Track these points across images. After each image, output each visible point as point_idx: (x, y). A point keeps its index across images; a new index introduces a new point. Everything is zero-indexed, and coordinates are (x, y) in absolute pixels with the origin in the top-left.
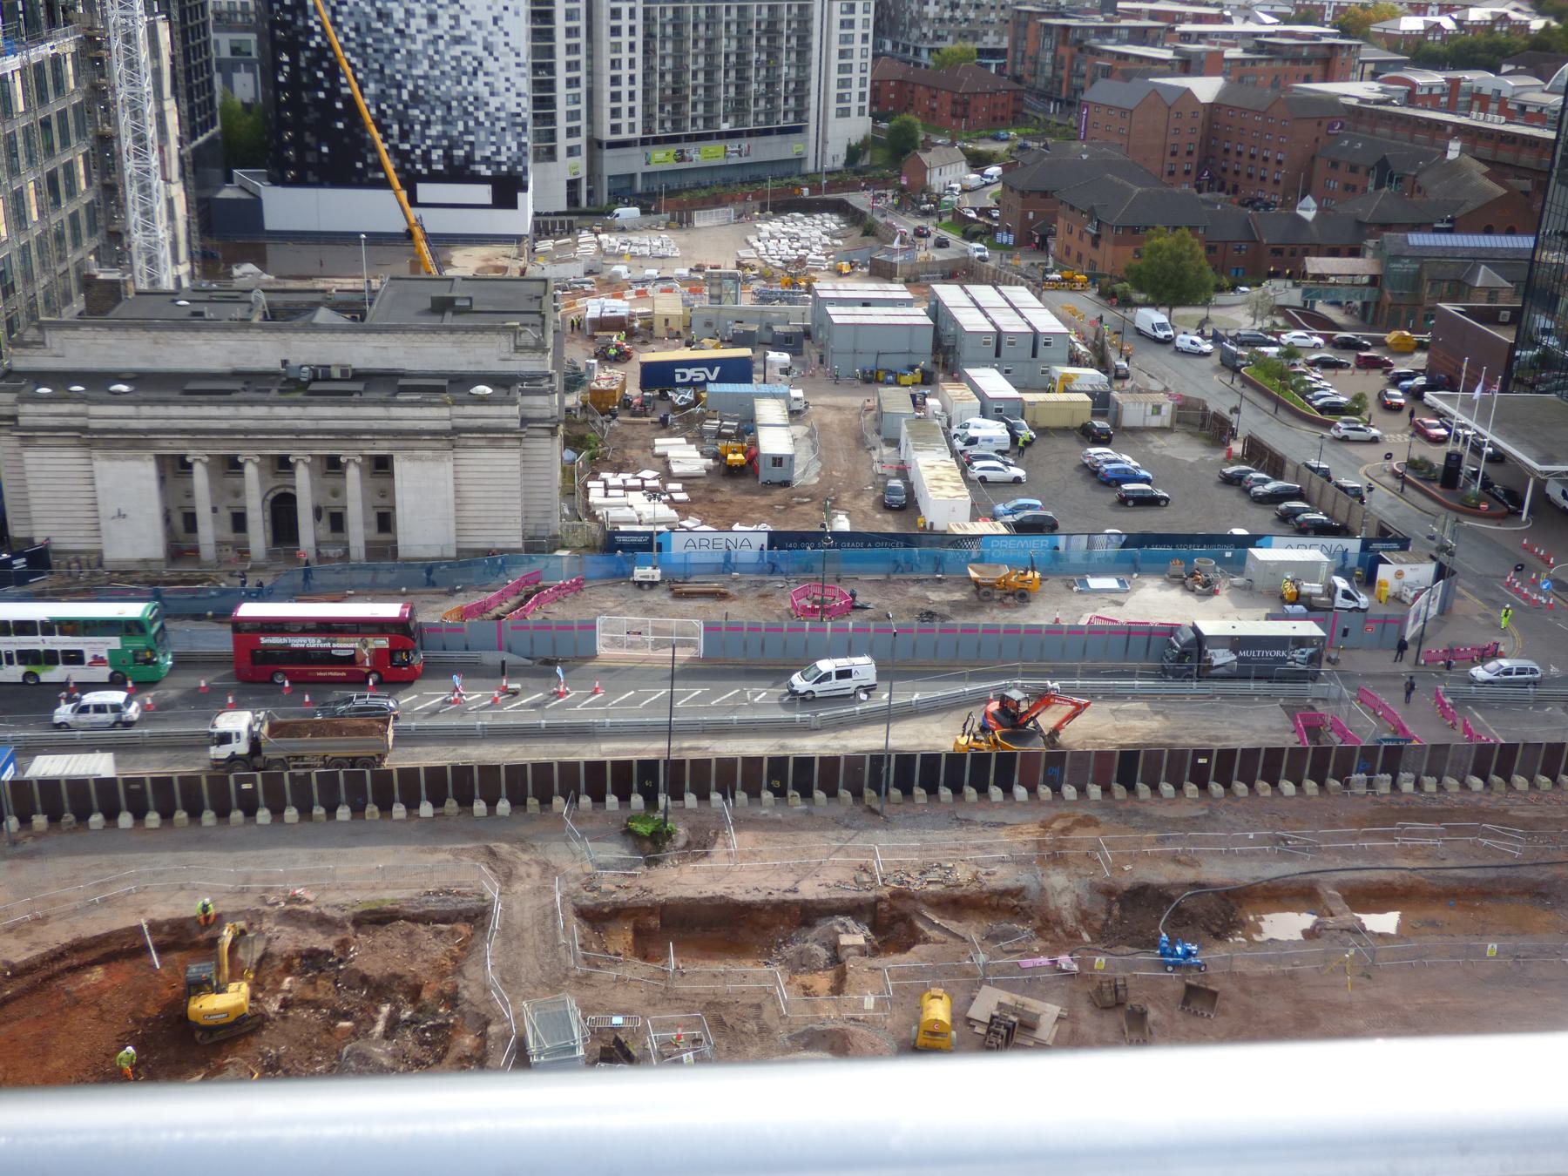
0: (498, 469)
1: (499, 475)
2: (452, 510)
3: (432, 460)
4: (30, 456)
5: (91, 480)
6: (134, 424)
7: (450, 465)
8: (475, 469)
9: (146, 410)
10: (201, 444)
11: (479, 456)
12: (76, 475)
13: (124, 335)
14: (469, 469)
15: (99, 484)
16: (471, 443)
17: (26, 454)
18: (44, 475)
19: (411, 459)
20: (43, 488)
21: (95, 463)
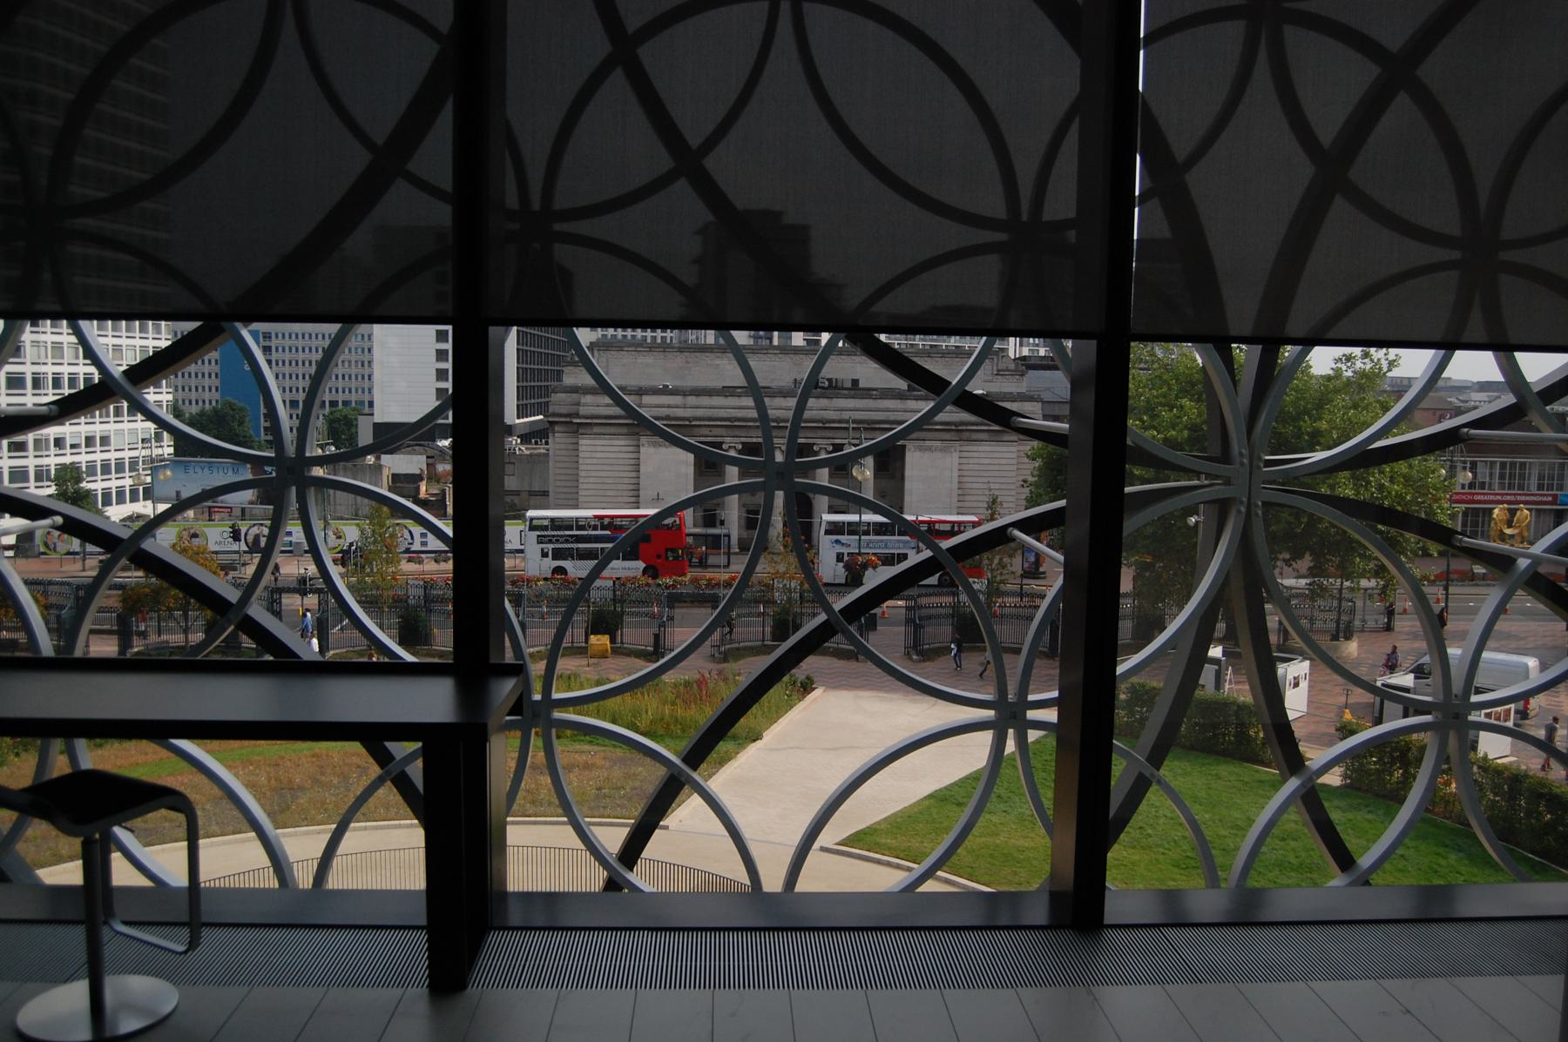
0: (997, 461)
1: (997, 468)
2: (955, 499)
3: (942, 450)
4: (585, 443)
5: (637, 467)
6: (680, 413)
7: (956, 455)
8: (976, 461)
9: (692, 400)
10: (737, 432)
11: (980, 448)
12: (621, 462)
13: (661, 355)
14: (971, 461)
15: (642, 469)
16: (975, 436)
17: (582, 442)
18: (595, 461)
19: (921, 449)
20: (593, 474)
21: (642, 450)
